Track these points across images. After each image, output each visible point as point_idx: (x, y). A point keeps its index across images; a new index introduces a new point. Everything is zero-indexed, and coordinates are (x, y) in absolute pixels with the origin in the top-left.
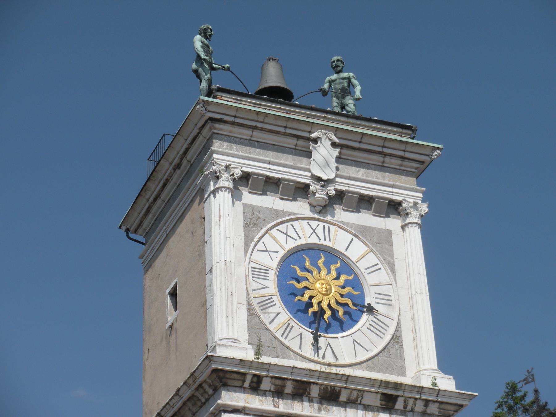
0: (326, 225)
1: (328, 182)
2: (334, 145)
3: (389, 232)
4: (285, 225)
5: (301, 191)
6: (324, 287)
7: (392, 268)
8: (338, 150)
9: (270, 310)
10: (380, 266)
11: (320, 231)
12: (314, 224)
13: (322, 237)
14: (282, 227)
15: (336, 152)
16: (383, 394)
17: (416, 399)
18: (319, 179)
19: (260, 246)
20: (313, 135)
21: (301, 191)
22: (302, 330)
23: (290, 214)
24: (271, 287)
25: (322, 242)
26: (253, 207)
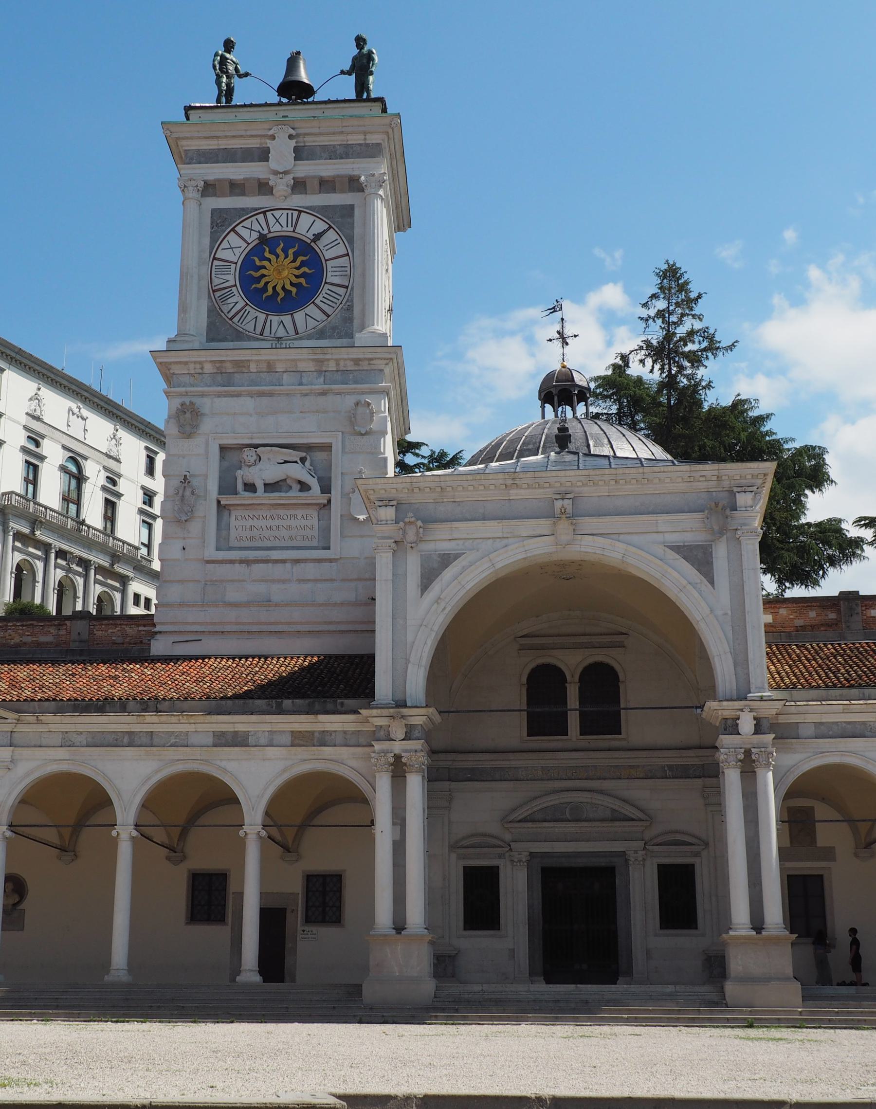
0: (290, 212)
1: (286, 173)
2: (291, 137)
3: (352, 207)
4: (250, 220)
5: (264, 188)
6: (281, 273)
7: (351, 240)
8: (294, 141)
9: (229, 301)
10: (339, 240)
11: (283, 220)
12: (277, 214)
13: (284, 225)
14: (247, 223)
15: (293, 143)
16: (313, 360)
17: (345, 360)
18: (276, 173)
19: (225, 244)
20: (271, 132)
21: (264, 188)
22: (258, 314)
23: (256, 209)
24: (231, 278)
25: (285, 229)
26: (220, 211)
